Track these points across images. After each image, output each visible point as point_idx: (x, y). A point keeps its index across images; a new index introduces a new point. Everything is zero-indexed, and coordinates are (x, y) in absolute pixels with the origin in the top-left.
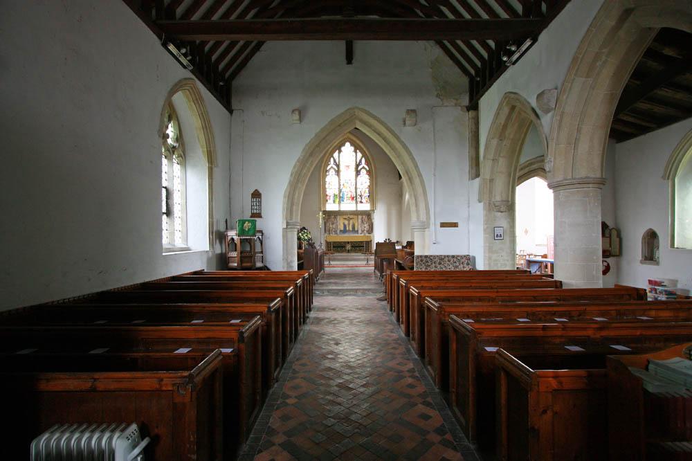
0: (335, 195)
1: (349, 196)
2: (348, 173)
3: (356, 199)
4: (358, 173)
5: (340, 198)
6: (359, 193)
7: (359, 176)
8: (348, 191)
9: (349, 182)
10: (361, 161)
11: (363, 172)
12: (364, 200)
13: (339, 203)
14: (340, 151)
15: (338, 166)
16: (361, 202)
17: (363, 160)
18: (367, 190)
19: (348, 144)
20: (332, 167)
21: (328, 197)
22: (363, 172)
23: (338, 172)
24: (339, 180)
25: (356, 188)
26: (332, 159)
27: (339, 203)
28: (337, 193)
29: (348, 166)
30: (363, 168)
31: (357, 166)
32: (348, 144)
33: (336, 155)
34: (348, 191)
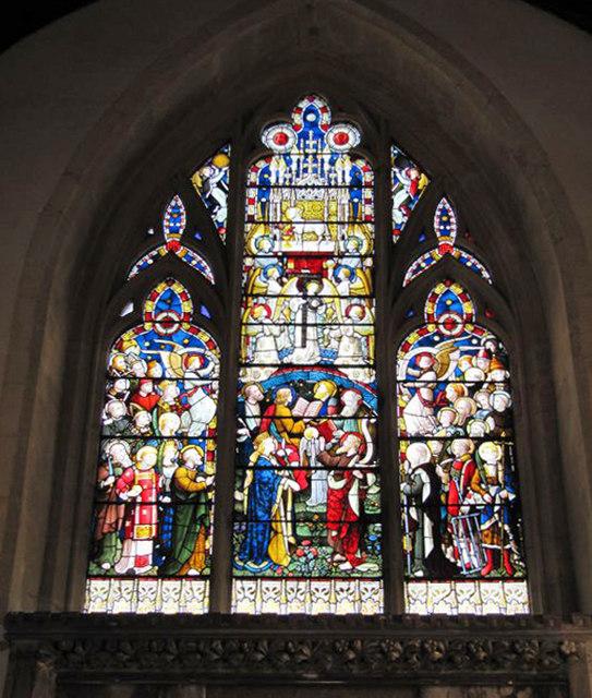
0: (179, 504)
1: (317, 499)
2: (309, 328)
3: (389, 542)
4: (397, 313)
5: (219, 519)
6: (415, 455)
7: (413, 338)
8: (313, 465)
9: (323, 390)
10: (421, 211)
11: (450, 304)
12: (467, 555)
13: (219, 579)
14: (248, 152)
15: (228, 251)
16: (441, 570)
17: (446, 225)
18: (491, 453)
19: (312, 108)
20: (171, 268)
21: (111, 516)
22: (450, 304)
23: (222, 311)
24: (233, 363)
25: (387, 439)
26: (174, 220)
27: (219, 579)
28: (196, 466)
29: (309, 267)
30: (447, 271)
31: (390, 254)
32: (312, 108)
33: (214, 176)
34: (313, 465)
